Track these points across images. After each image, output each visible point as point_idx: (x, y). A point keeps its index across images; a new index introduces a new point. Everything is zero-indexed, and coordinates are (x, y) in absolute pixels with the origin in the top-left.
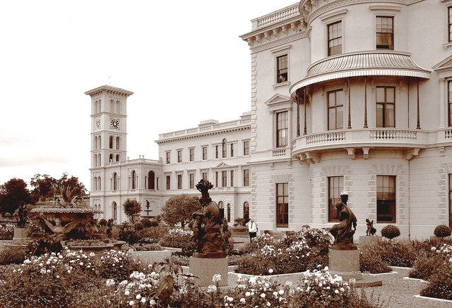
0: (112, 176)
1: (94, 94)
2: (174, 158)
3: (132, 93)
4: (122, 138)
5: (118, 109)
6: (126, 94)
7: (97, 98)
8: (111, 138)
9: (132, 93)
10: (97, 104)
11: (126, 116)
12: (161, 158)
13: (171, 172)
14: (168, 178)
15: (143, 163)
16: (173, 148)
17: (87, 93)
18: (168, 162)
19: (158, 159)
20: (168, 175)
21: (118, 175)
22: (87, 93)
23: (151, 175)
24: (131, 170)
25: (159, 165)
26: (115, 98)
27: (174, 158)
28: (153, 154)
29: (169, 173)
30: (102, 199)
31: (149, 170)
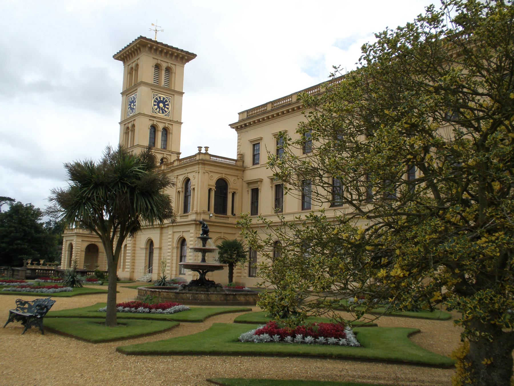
3: (193, 56)
4: (174, 129)
5: (169, 80)
8: (154, 128)
9: (193, 56)
10: (132, 72)
11: (182, 93)
12: (241, 156)
13: (261, 181)
14: (255, 193)
15: (203, 160)
16: (266, 134)
18: (255, 162)
19: (235, 158)
20: (254, 186)
25: (238, 166)
29: (256, 182)
31: (216, 177)
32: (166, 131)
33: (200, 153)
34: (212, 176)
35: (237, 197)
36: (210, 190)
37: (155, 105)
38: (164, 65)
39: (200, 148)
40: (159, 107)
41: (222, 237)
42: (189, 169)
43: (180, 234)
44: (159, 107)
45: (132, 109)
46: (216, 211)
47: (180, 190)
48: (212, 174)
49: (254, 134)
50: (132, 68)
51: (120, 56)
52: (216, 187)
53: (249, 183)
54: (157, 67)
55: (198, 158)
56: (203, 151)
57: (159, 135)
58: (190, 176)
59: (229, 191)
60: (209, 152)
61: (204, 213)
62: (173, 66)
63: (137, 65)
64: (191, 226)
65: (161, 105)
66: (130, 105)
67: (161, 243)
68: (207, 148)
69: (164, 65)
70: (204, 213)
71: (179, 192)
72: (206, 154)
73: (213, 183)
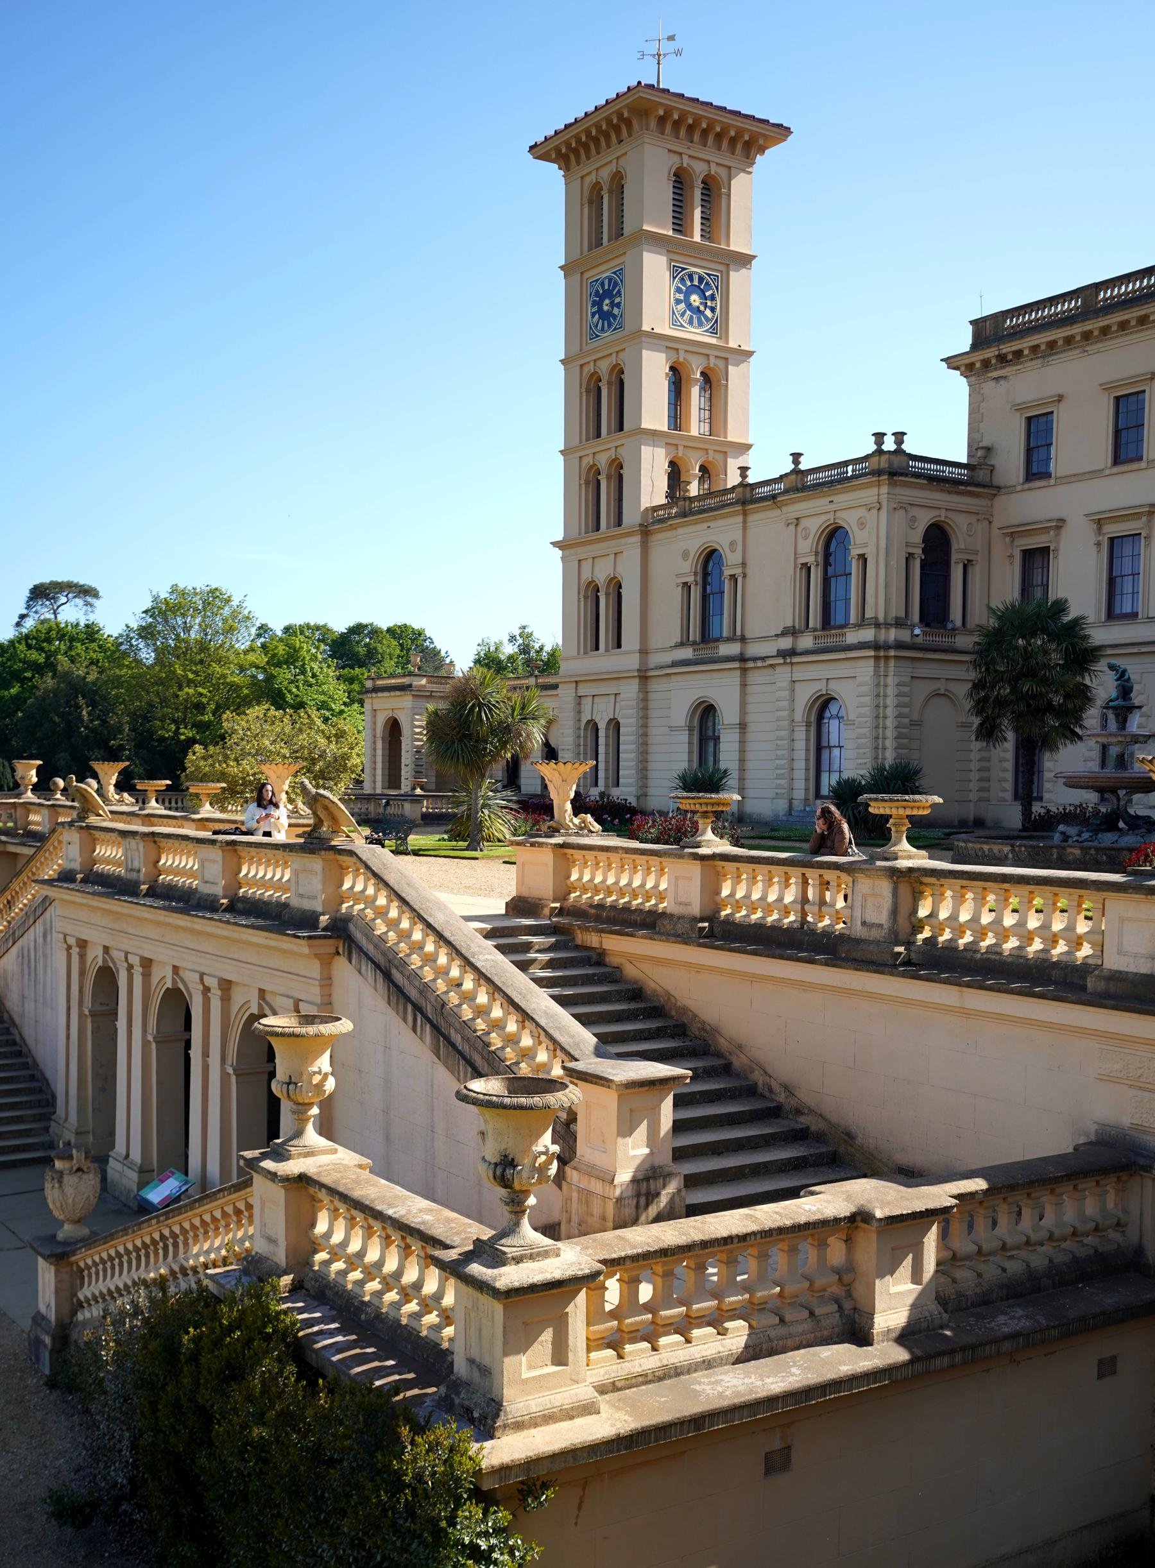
0: (687, 569)
1: (567, 148)
2: (1082, 438)
3: (782, 132)
6: (748, 137)
7: (600, 168)
9: (782, 132)
17: (539, 151)
18: (1037, 468)
19: (964, 460)
21: (731, 560)
22: (539, 151)
23: (937, 541)
24: (814, 526)
26: (702, 161)
27: (1082, 438)
28: (942, 430)
30: (630, 690)
31: (925, 519)
32: (708, 380)
33: (879, 452)
34: (914, 519)
35: (976, 573)
36: (909, 557)
37: (678, 302)
38: (699, 170)
39: (879, 437)
40: (689, 305)
41: (942, 692)
42: (842, 499)
43: (820, 687)
44: (689, 305)
45: (606, 316)
46: (924, 620)
47: (810, 559)
48: (914, 511)
49: (1030, 383)
50: (597, 187)
51: (557, 150)
52: (924, 550)
53: (1013, 535)
54: (680, 180)
55: (874, 463)
56: (889, 445)
57: (695, 396)
58: (849, 520)
59: (954, 556)
60: (907, 447)
61: (899, 623)
62: (722, 172)
63: (618, 179)
64: (862, 663)
65: (695, 299)
66: (599, 304)
67: (743, 712)
68: (899, 437)
69: (699, 170)
70: (899, 623)
71: (807, 568)
72: (899, 452)
73: (917, 537)
